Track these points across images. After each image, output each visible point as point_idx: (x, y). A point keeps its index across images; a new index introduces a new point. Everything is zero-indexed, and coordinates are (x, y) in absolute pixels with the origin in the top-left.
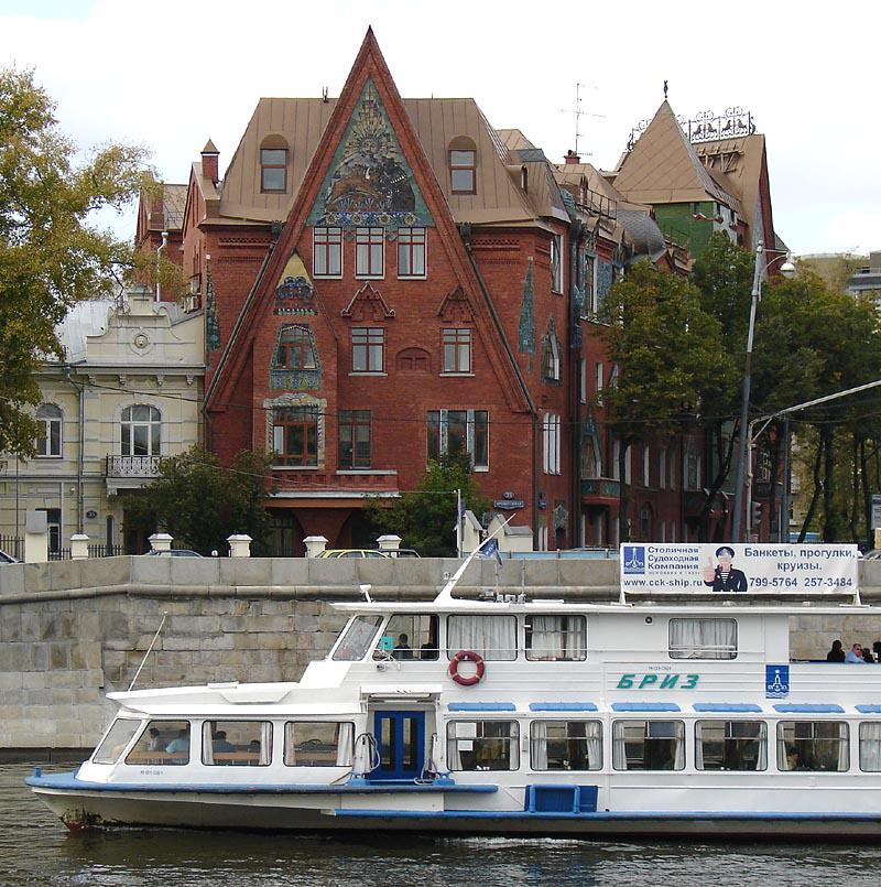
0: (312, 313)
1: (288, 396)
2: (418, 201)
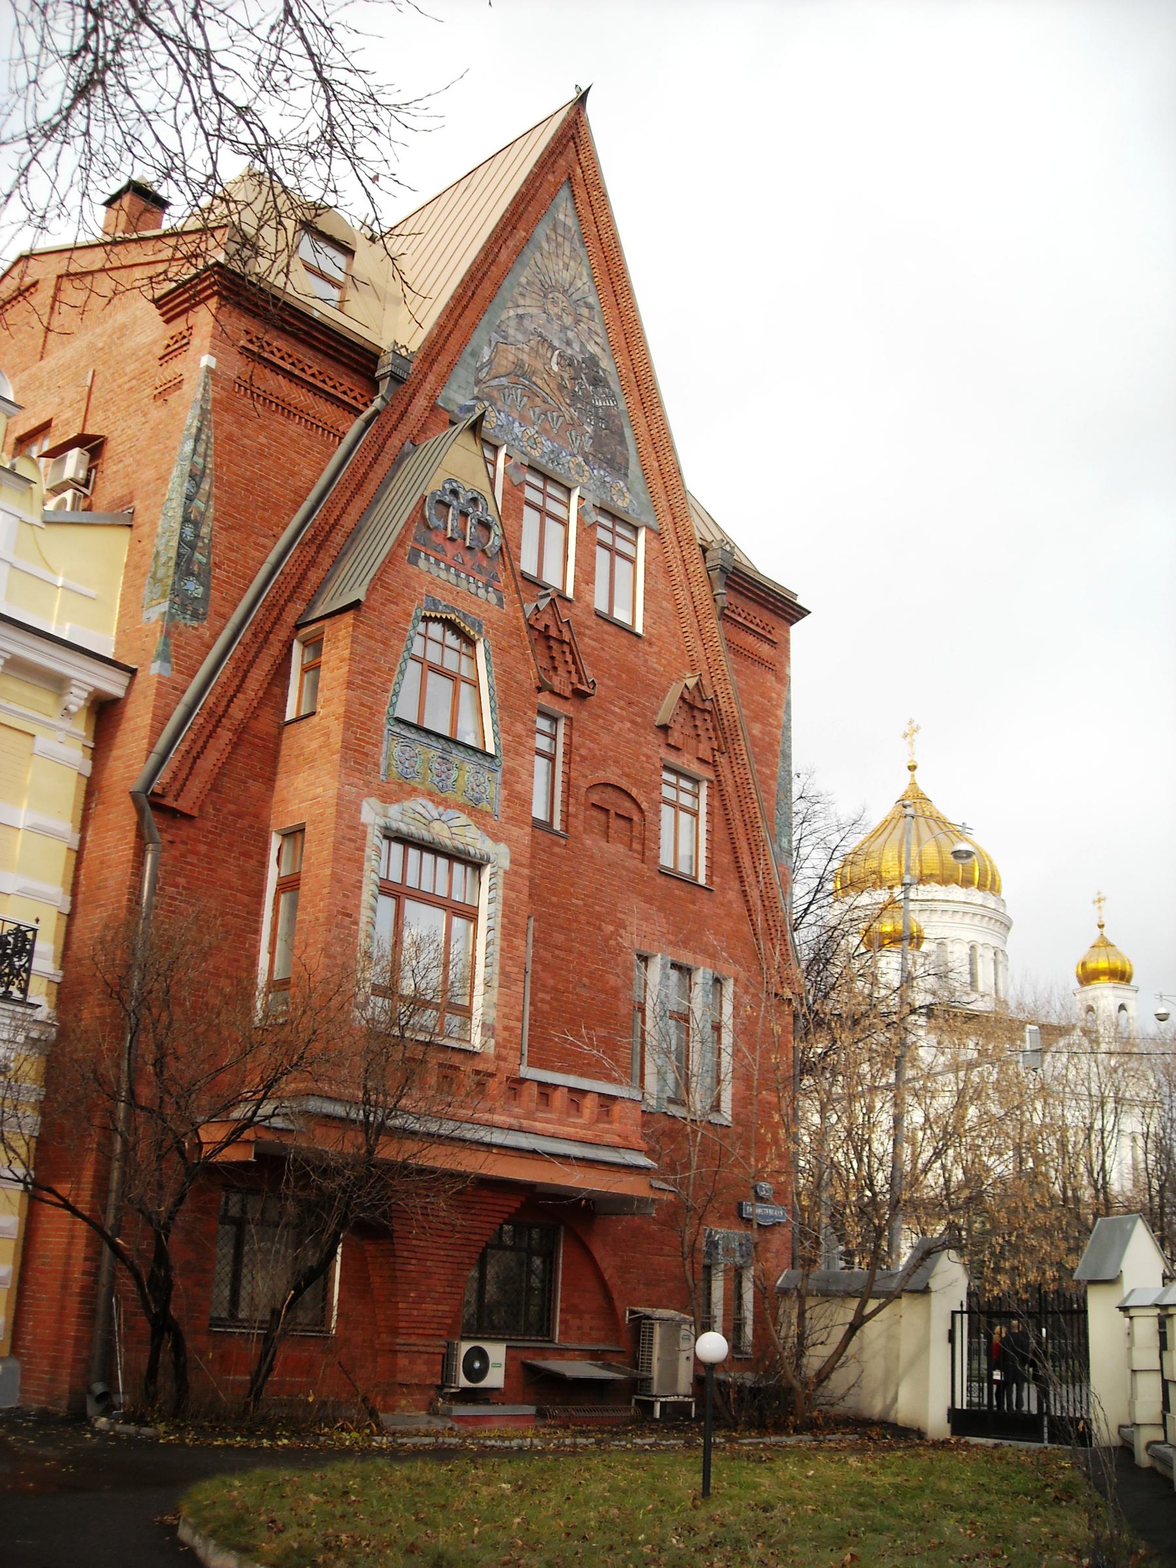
0: (493, 598)
1: (421, 805)
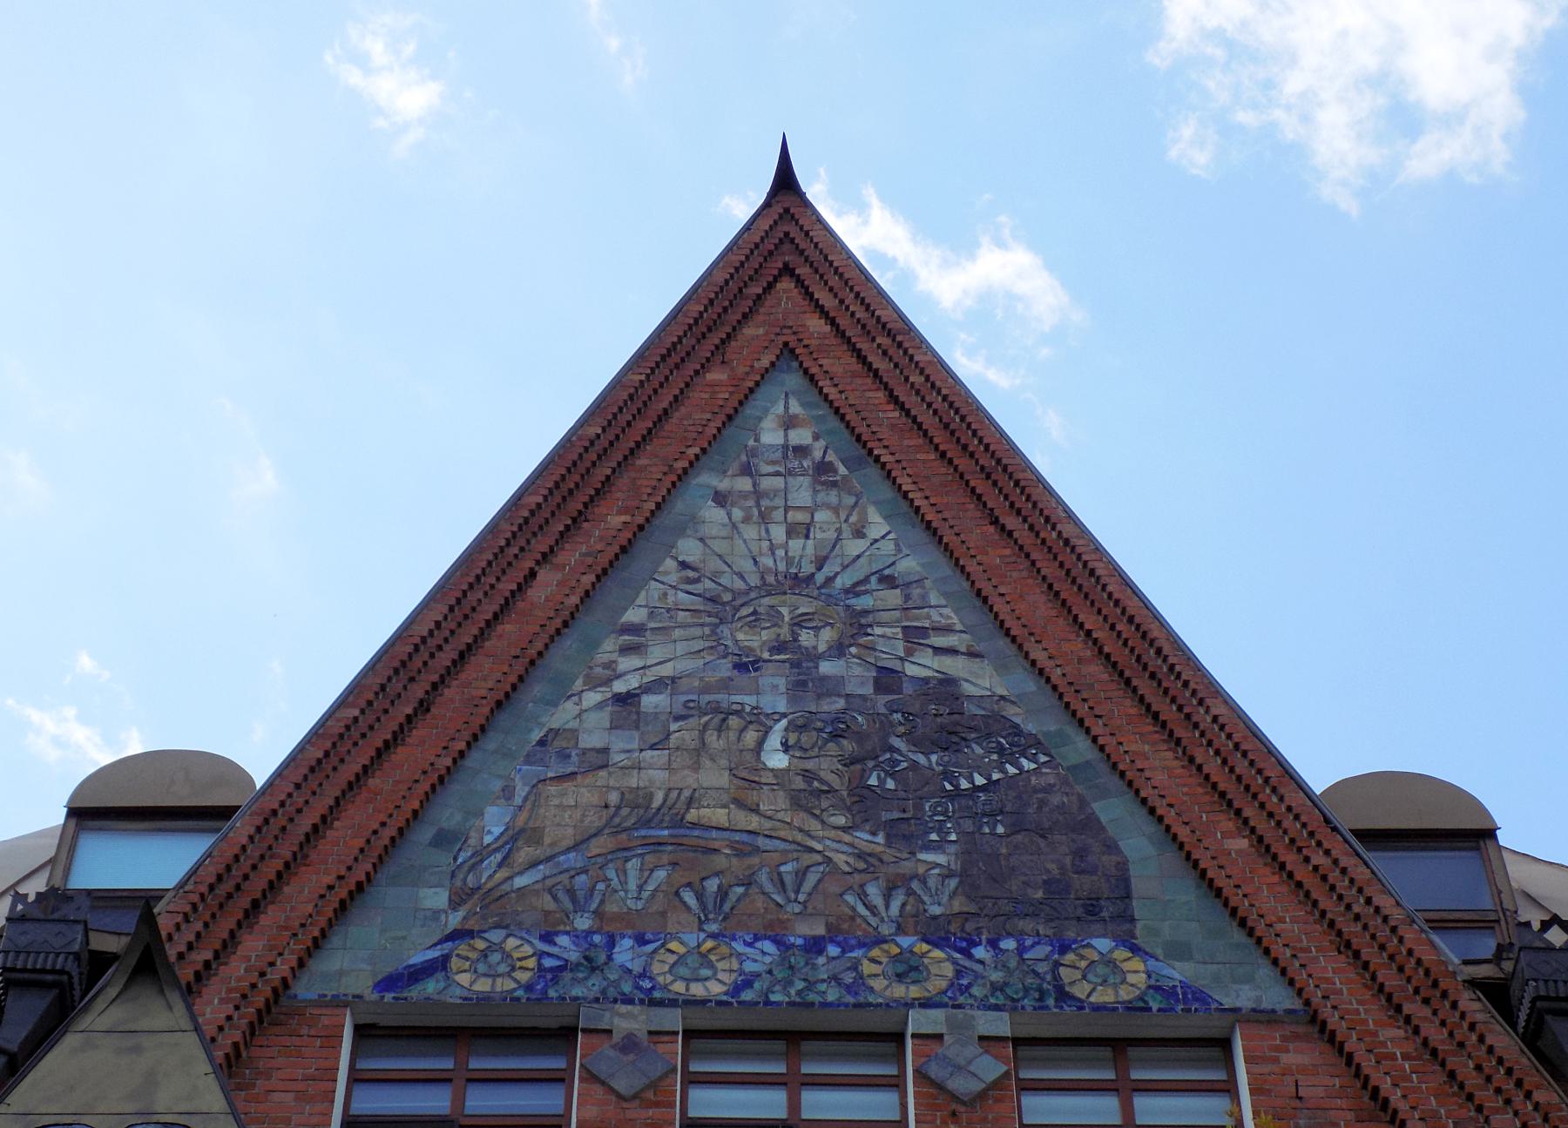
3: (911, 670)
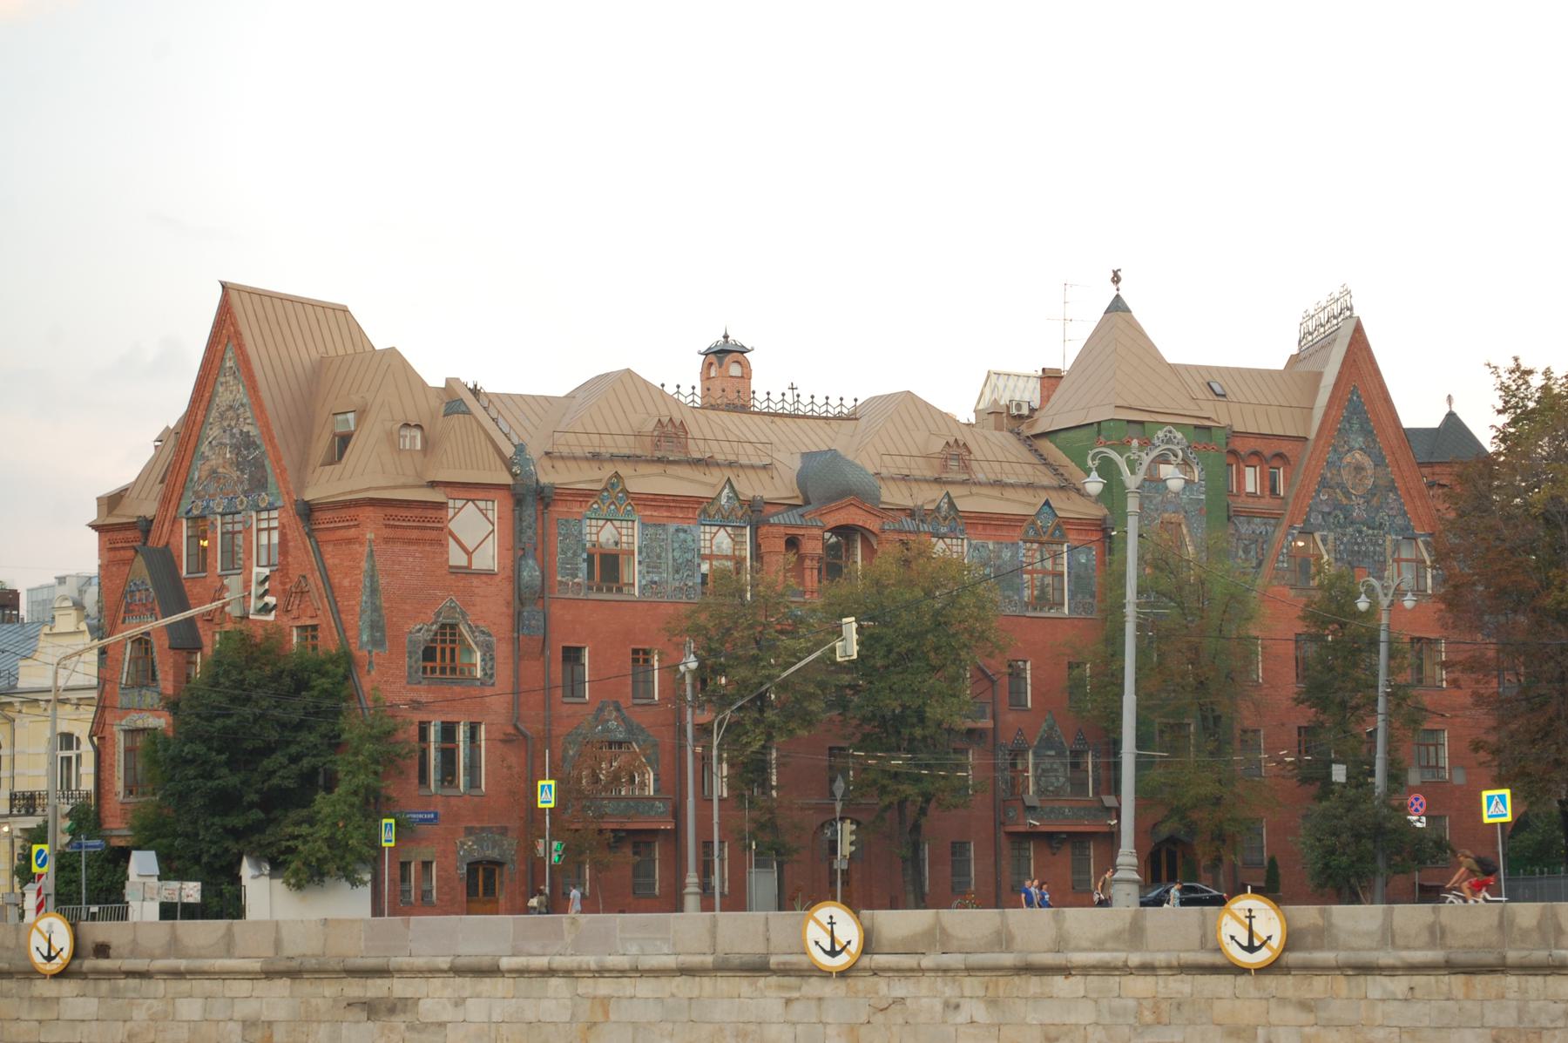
1: (135, 716)
2: (271, 479)
3: (245, 430)
